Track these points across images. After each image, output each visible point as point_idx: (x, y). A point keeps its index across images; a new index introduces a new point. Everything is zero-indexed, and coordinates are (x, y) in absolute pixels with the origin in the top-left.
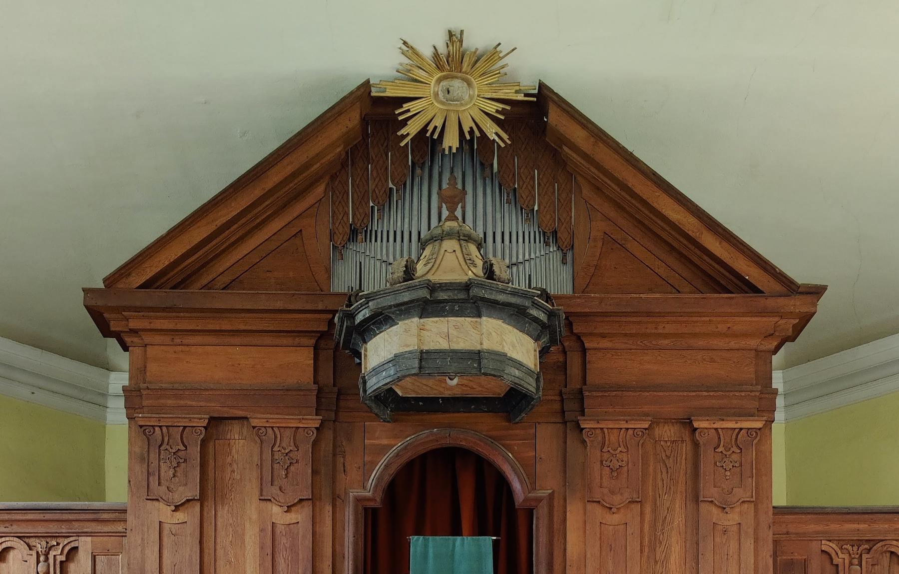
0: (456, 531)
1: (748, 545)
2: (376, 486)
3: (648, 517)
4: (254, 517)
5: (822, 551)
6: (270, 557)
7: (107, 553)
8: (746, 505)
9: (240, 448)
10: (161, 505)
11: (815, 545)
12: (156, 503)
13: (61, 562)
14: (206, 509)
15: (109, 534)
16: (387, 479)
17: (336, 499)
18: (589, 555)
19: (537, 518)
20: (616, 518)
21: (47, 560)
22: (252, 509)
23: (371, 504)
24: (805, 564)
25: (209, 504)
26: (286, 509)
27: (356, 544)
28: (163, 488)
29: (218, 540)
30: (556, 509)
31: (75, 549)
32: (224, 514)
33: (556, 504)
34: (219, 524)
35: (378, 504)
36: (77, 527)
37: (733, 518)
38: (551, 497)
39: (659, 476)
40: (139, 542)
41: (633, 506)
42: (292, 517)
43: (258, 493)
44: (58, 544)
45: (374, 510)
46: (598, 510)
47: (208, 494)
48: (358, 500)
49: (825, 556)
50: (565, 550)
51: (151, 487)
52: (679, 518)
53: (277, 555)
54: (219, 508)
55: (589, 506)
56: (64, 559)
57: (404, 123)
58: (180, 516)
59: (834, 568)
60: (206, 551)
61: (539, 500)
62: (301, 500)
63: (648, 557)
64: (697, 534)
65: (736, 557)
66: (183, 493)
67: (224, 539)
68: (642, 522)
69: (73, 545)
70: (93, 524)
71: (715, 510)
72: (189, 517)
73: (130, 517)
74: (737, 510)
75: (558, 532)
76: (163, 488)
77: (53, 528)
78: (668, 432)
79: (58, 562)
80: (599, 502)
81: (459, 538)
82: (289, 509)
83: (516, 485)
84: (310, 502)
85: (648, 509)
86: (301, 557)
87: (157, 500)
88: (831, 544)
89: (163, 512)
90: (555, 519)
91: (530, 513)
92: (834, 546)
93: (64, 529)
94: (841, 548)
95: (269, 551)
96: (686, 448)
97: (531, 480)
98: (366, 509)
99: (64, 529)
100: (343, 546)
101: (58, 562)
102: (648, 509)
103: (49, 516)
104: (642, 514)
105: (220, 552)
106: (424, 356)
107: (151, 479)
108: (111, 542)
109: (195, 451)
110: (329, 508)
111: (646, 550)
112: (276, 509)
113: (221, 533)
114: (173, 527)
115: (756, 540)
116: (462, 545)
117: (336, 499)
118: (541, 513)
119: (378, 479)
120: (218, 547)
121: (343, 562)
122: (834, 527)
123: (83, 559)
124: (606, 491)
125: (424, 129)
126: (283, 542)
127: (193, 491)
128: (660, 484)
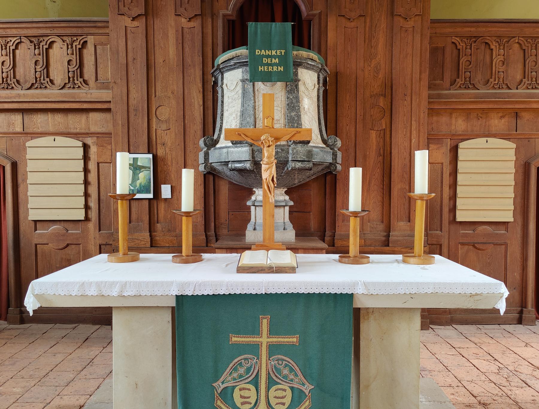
0: (273, 20)
1: (418, 38)
2: (233, 8)
3: (368, 24)
4: (173, 24)
5: (452, 42)
6: (181, 45)
7: (102, 44)
8: (417, 17)
10: (126, 18)
11: (449, 39)
12: (123, 17)
13: (79, 48)
14: (148, 20)
15: (101, 34)
16: (239, 5)
17: (213, 16)
18: (339, 43)
19: (313, 25)
20: (353, 24)
21: (72, 47)
22: (171, 20)
23: (231, 18)
24: (444, 49)
25: (150, 17)
26: (188, 20)
27: (223, 38)
28: (126, 8)
29: (155, 36)
30: (322, 20)
31: (86, 42)
33: (322, 18)
34: (155, 28)
35: (234, 18)
36: (86, 30)
37: (411, 23)
38: (320, 14)
39: (374, 3)
40: (116, 37)
41: (361, 18)
42: (192, 24)
43: (173, 11)
44: (77, 39)
45: (233, 21)
46: (343, 20)
48: (224, 16)
49: (454, 45)
50: (327, 41)
51: (120, 8)
52: (383, 25)
53: (185, 44)
54: (155, 19)
55: (339, 18)
56: (80, 47)
58: (136, 23)
59: (457, 51)
60: (149, 42)
61: (314, 15)
62: (196, 15)
63: (368, 44)
64: (392, 32)
65: (411, 43)
66: (136, 11)
67: (158, 36)
68: (365, 27)
69: (85, 40)
70: (94, 29)
71: (402, 20)
72: (140, 23)
73: (110, 24)
74: (413, 19)
76: (126, 8)
77: (74, 31)
79: (78, 49)
80: (344, 16)
81: (274, 23)
82: (190, 20)
83: (303, 8)
84: (201, 16)
85: (368, 20)
86: (196, 45)
87: (123, 15)
88: (457, 39)
89: (127, 21)
90: (322, 25)
91: (309, 22)
92: (458, 39)
93: (80, 31)
94: (462, 41)
95: (181, 42)
97: (310, 5)
98: (229, 21)
99: (80, 31)
100: (217, 39)
101: (78, 49)
102: (368, 20)
103: (72, 25)
104: (365, 22)
105: (156, 42)
107: (120, 3)
108: (103, 38)
110: (210, 20)
111: (367, 41)
112: (183, 20)
113: (157, 33)
114: (132, 29)
115: (422, 35)
116: (276, 27)
118: (316, 21)
119: (234, 5)
120: (155, 40)
121: (217, 48)
122: (459, 30)
123: (90, 47)
124: (347, 10)
126: (187, 37)
128: (374, 7)
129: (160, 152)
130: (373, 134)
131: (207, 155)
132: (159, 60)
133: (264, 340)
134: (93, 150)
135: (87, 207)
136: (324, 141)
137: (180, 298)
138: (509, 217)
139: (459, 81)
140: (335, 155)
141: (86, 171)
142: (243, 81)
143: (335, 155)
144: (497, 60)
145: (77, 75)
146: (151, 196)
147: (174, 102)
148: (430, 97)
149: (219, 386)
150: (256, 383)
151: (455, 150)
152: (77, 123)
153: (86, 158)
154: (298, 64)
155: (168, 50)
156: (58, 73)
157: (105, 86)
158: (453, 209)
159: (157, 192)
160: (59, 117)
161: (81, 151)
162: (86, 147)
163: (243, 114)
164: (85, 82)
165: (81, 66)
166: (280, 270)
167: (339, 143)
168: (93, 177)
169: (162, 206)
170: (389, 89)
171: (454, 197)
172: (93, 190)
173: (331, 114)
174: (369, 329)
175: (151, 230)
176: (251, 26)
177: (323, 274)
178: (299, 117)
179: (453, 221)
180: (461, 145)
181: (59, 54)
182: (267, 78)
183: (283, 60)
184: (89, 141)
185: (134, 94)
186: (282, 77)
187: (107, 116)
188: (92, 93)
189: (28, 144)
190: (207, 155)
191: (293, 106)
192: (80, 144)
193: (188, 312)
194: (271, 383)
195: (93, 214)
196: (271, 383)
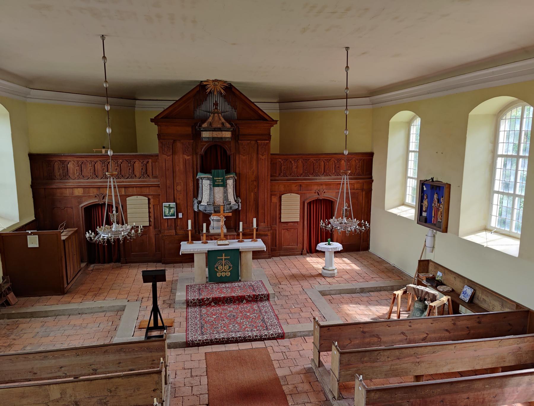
1: (266, 162)
9: (179, 145)
22: (181, 156)
32: (176, 157)
37: (263, 158)
42: (188, 158)
47: (174, 153)
57: (207, 89)
75: (235, 160)
78: (253, 142)
96: (256, 145)
106: (213, 138)
109: (171, 146)
117: (196, 154)
125: (211, 91)
126: (187, 162)
127: (171, 153)
129: (178, 202)
130: (252, 194)
131: (198, 206)
132: (177, 169)
133: (224, 258)
134: (152, 200)
135: (150, 221)
136: (235, 201)
137: (208, 251)
138: (298, 220)
139: (282, 174)
140: (239, 205)
141: (149, 208)
142: (210, 185)
143: (239, 205)
144: (294, 167)
145: (145, 173)
146: (175, 217)
147: (182, 184)
148: (271, 180)
149: (216, 266)
150: (222, 265)
151: (280, 197)
152: (146, 191)
153: (149, 203)
154: (226, 180)
155: (180, 167)
156: (137, 173)
157: (156, 177)
158: (280, 218)
159: (177, 215)
160: (138, 189)
161: (147, 201)
162: (149, 200)
163: (210, 195)
164: (148, 176)
165: (146, 170)
166: (226, 245)
167: (240, 201)
168: (152, 210)
169: (179, 220)
170: (257, 179)
171: (280, 214)
172: (152, 215)
173: (238, 187)
174: (243, 255)
175: (175, 229)
176: (213, 171)
177: (234, 244)
178: (227, 195)
179: (280, 222)
180: (282, 196)
181: (138, 165)
182: (218, 186)
183: (223, 181)
184: (150, 197)
185: (168, 182)
186: (221, 186)
187: (157, 188)
188: (152, 181)
189: (127, 199)
190: (198, 206)
191: (226, 192)
192: (147, 198)
193: (209, 254)
194: (225, 265)
195: (152, 224)
196: (225, 265)
